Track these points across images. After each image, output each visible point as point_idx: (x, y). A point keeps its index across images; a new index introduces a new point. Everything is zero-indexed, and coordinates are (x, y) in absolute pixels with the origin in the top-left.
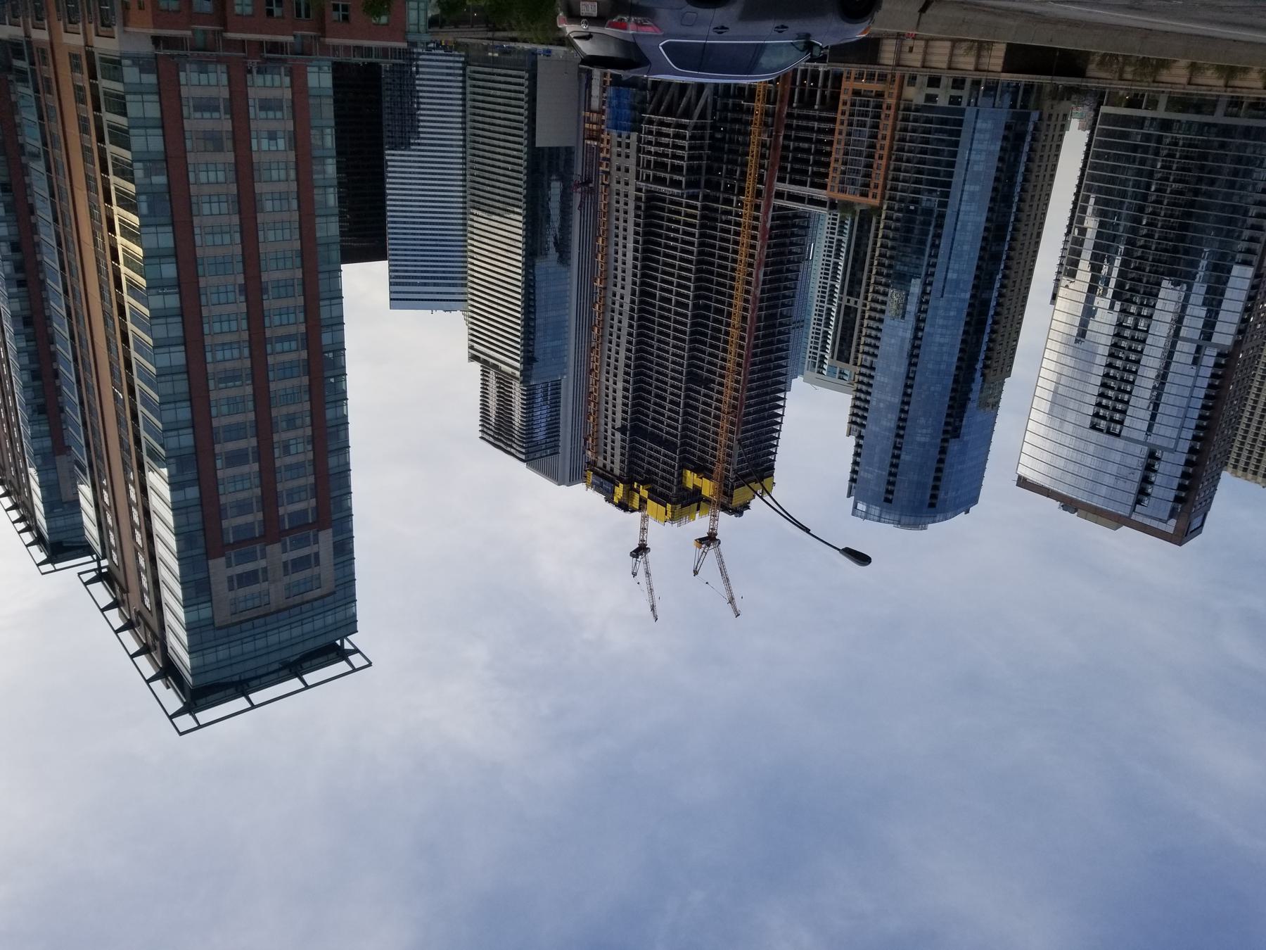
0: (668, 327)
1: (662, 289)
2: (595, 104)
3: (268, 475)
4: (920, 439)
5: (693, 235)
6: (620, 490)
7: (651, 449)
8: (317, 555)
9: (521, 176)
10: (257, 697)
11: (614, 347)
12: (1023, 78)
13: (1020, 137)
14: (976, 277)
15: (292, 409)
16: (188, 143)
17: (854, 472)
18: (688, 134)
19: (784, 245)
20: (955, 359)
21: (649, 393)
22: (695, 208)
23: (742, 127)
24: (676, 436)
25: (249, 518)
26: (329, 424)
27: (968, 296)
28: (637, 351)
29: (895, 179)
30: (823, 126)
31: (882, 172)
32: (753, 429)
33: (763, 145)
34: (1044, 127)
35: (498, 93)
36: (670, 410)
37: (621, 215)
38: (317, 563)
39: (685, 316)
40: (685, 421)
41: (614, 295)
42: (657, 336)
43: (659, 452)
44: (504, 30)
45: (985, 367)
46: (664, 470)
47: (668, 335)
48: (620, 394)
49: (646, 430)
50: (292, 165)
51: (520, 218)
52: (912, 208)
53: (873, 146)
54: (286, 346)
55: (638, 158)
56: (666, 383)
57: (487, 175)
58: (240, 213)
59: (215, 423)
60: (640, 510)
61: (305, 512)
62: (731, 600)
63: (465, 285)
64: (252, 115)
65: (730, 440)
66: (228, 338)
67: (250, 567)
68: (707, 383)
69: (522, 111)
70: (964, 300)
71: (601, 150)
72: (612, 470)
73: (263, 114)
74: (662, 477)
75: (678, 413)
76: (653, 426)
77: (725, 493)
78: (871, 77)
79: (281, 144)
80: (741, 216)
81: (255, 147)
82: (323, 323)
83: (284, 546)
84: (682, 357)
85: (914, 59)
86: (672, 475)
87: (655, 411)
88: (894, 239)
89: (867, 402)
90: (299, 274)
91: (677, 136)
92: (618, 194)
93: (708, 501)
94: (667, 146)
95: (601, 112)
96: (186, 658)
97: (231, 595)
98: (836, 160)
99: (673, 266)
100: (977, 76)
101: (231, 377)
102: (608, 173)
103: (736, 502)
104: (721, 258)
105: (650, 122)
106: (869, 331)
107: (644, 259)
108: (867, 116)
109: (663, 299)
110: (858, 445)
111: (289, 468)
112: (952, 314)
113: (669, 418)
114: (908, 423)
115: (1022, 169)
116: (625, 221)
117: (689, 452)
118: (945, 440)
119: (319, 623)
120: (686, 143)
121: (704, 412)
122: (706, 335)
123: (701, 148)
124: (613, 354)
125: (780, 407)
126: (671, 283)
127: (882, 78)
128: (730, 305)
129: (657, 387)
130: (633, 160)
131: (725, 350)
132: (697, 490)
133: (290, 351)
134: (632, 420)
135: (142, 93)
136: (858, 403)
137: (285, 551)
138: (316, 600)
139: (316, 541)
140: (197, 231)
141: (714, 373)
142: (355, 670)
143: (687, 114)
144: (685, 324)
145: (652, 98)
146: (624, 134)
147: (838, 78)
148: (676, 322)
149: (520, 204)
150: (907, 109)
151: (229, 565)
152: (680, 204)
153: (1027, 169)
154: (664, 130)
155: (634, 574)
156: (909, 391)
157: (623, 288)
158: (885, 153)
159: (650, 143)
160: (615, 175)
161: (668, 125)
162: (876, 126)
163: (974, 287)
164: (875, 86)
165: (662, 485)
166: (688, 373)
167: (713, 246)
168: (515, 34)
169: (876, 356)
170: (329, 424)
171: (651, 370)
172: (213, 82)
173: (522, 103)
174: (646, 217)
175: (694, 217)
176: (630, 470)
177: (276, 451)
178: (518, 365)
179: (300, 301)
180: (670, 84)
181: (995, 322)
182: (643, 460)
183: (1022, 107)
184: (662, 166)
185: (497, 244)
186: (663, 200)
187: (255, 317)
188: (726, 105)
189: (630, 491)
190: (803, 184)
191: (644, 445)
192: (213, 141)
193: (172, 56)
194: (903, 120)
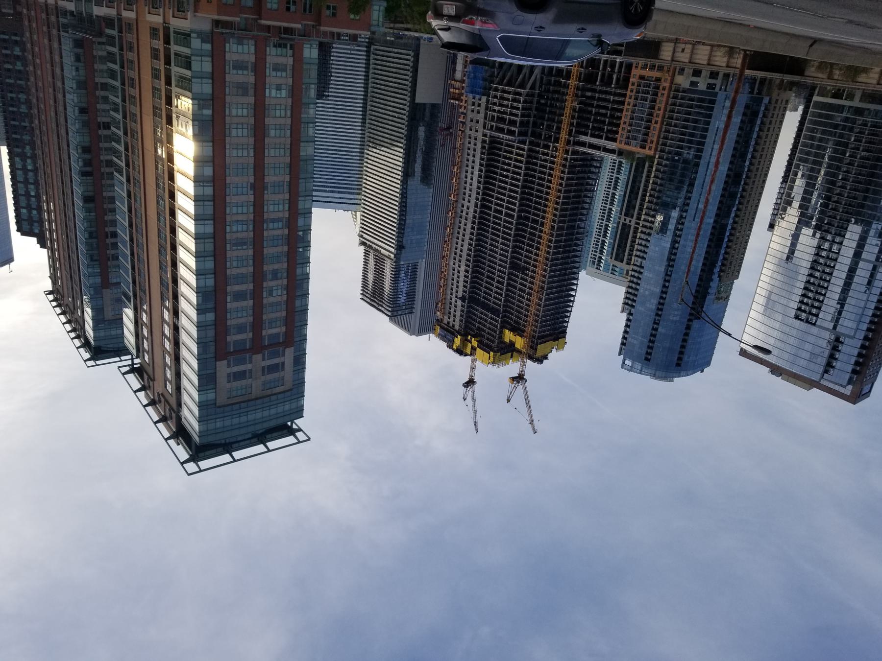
0: (499, 230)
1: (497, 204)
2: (458, 75)
3: (258, 310)
4: (671, 318)
5: (520, 168)
6: (458, 340)
7: (482, 313)
8: (283, 363)
9: (404, 122)
10: (237, 454)
11: (460, 241)
12: (760, 74)
13: (755, 114)
14: (719, 209)
15: (276, 266)
16: (227, 89)
17: (624, 338)
18: (522, 99)
19: (583, 178)
20: (701, 264)
22: (523, 150)
23: (560, 97)
24: (500, 306)
25: (243, 336)
26: (298, 278)
27: (712, 221)
28: (476, 245)
29: (666, 138)
30: (616, 98)
31: (657, 133)
33: (574, 110)
34: (772, 108)
35: (392, 65)
36: (497, 287)
37: (471, 152)
38: (283, 369)
39: (511, 223)
40: (507, 295)
41: (463, 206)
42: (490, 236)
43: (487, 316)
44: (402, 23)
45: (721, 271)
46: (489, 329)
47: (498, 236)
48: (462, 274)
49: (479, 300)
50: (289, 107)
51: (402, 150)
53: (651, 114)
54: (276, 225)
55: (486, 114)
57: (380, 120)
58: (255, 136)
59: (228, 272)
60: (471, 355)
61: (278, 334)
62: (532, 422)
63: (359, 194)
64: (268, 74)
65: (538, 310)
66: (240, 218)
67: (241, 368)
68: (524, 270)
69: (407, 78)
70: (709, 224)
71: (461, 107)
72: (453, 326)
73: (274, 73)
74: (488, 333)
75: (502, 290)
76: (484, 298)
77: (532, 347)
78: (653, 67)
79: (284, 92)
80: (555, 157)
81: (267, 95)
82: (300, 212)
83: (264, 356)
84: (508, 252)
85: (684, 57)
86: (495, 332)
87: (486, 287)
88: (662, 179)
89: (637, 290)
90: (287, 178)
91: (514, 100)
92: (470, 138)
93: (519, 352)
94: (507, 106)
95: (463, 81)
96: (196, 425)
97: (228, 385)
98: (625, 123)
99: (505, 189)
100: (728, 70)
101: (240, 243)
102: (463, 123)
103: (539, 354)
104: (539, 184)
105: (496, 90)
106: (640, 241)
107: (485, 183)
109: (496, 211)
110: (628, 320)
111: (272, 305)
113: (496, 292)
114: (665, 306)
115: (755, 136)
116: (474, 156)
117: (508, 317)
118: (690, 320)
119: (280, 409)
120: (520, 106)
121: (520, 290)
122: (525, 237)
123: (530, 109)
124: (459, 246)
125: (573, 290)
126: (503, 200)
127: (661, 68)
128: (543, 218)
129: (488, 271)
130: (482, 115)
131: (538, 249)
132: (512, 344)
133: (278, 229)
134: (470, 292)
135: (201, 56)
136: (630, 290)
137: (264, 359)
138: (280, 393)
139: (284, 355)
140: (228, 146)
141: (529, 264)
142: (299, 442)
143: (522, 86)
144: (511, 229)
145: (498, 74)
146: (478, 97)
147: (629, 67)
148: (504, 227)
149: (402, 141)
150: (677, 90)
151: (229, 366)
152: (513, 147)
153: (759, 137)
154: (506, 95)
155: (465, 399)
156: (667, 284)
157: (469, 202)
158: (659, 120)
159: (495, 104)
160: (469, 124)
161: (509, 93)
162: (654, 101)
163: (717, 215)
164: (656, 74)
165: (488, 339)
166: (511, 263)
167: (534, 177)
168: (409, 26)
170: (298, 278)
171: (485, 259)
172: (246, 51)
173: (409, 73)
174: (488, 154)
175: (522, 156)
176: (466, 326)
177: (265, 293)
178: (393, 250)
179: (287, 196)
180: (511, 65)
181: (729, 241)
182: (475, 320)
183: (758, 94)
184: (501, 120)
185: (385, 166)
186: (501, 144)
187: (258, 206)
188: (550, 81)
189: (465, 341)
190: (600, 137)
191: (477, 310)
192: (242, 89)
193: (222, 33)
194: (673, 98)
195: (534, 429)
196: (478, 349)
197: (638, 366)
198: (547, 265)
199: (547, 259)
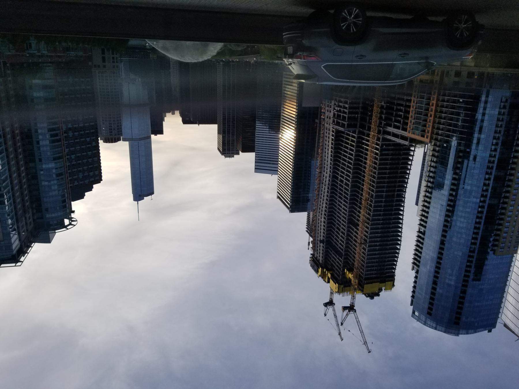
6: (320, 270)
17: (414, 292)
21: (335, 226)
22: (354, 137)
24: (342, 250)
27: (478, 200)
32: (378, 254)
33: (382, 107)
43: (336, 256)
46: (337, 266)
49: (333, 244)
52: (445, 145)
53: (427, 110)
56: (340, 222)
60: (329, 282)
70: (476, 203)
86: (340, 269)
88: (436, 162)
91: (346, 103)
98: (412, 117)
102: (324, 119)
108: (424, 93)
110: (416, 277)
123: (358, 108)
132: (350, 280)
134: (327, 237)
158: (433, 113)
165: (336, 274)
166: (349, 219)
169: (425, 227)
184: (339, 116)
190: (397, 127)
197: (423, 318)
198: (368, 224)
199: (368, 219)
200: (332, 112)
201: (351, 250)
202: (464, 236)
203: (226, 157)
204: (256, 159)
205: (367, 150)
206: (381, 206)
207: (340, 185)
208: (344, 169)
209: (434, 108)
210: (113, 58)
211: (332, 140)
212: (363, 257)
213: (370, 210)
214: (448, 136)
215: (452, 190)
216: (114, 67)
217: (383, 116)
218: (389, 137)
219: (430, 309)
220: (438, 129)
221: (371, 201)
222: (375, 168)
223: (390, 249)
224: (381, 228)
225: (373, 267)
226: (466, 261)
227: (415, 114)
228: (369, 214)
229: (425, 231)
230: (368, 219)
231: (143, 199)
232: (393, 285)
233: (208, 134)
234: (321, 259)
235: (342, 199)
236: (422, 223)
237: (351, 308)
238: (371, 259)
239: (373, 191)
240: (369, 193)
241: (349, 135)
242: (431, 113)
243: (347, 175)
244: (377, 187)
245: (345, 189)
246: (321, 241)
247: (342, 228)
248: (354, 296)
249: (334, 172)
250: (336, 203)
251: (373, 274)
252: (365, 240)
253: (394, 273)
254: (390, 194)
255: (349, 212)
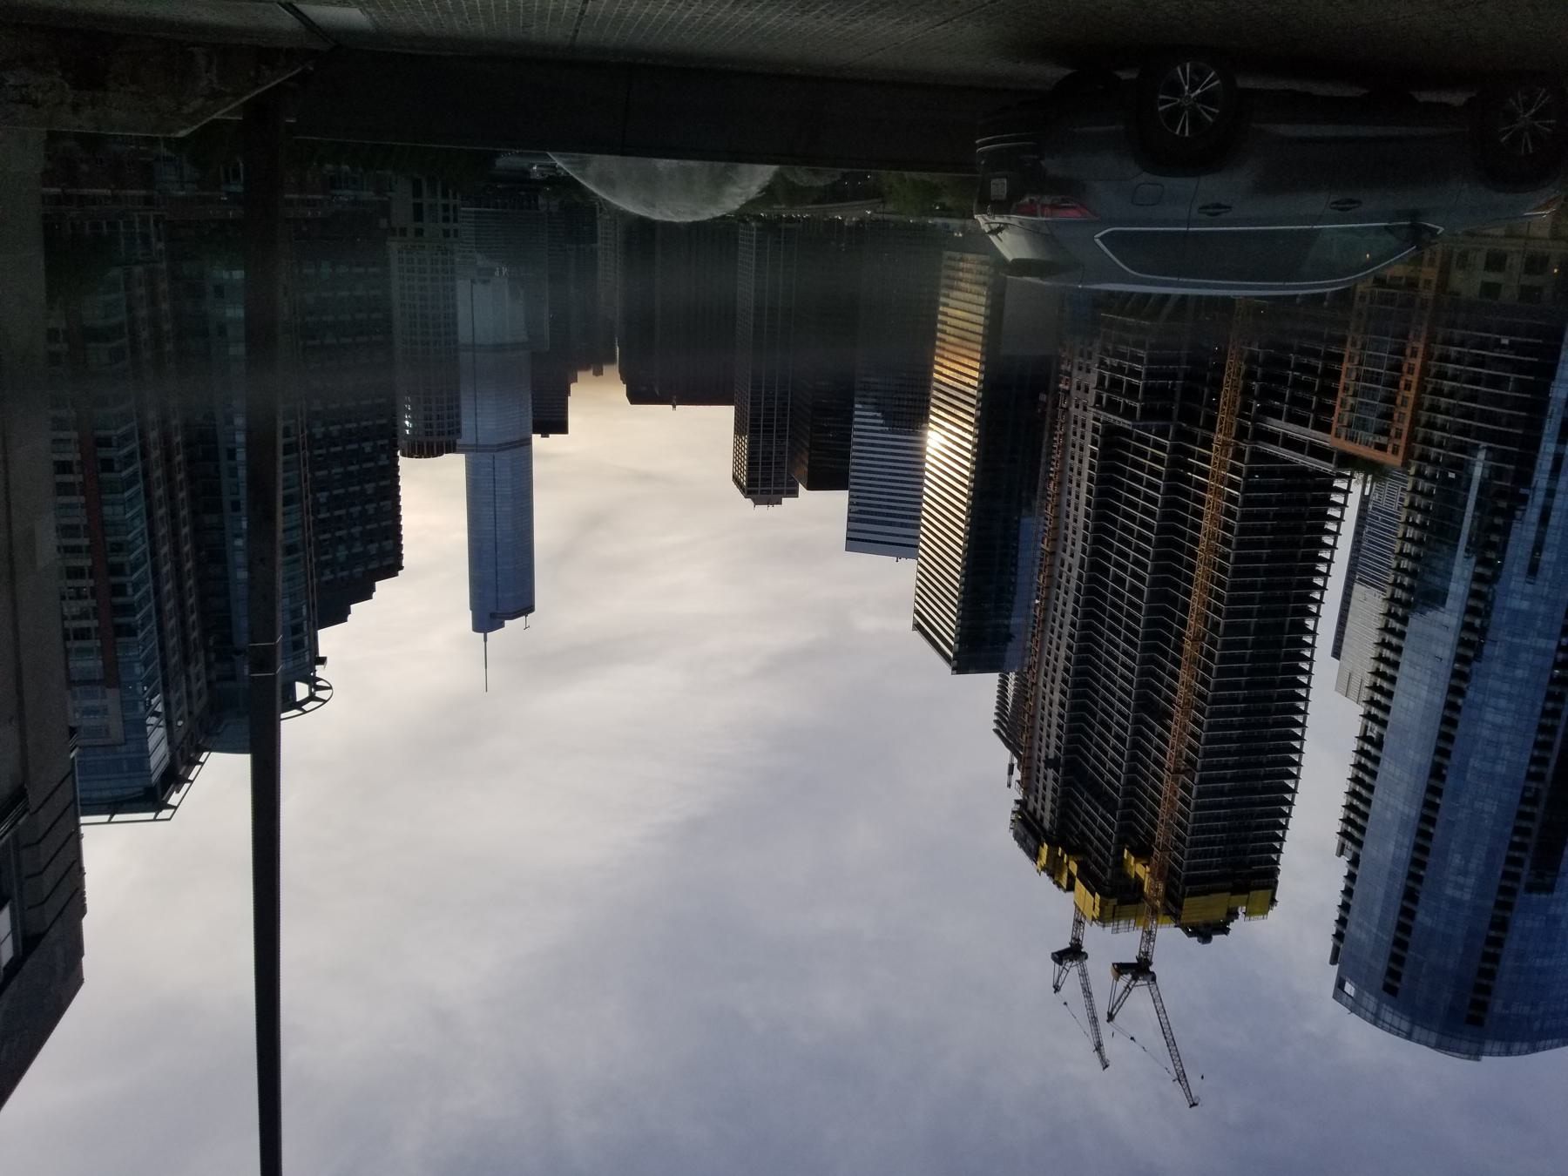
6: (1044, 850)
17: (1342, 922)
21: (1094, 715)
22: (1162, 448)
24: (1116, 790)
27: (1553, 645)
31: (1408, 412)
33: (1252, 359)
43: (1096, 810)
52: (1452, 475)
53: (1397, 367)
56: (1112, 706)
60: (1071, 888)
72: (1042, 818)
86: (1108, 849)
98: (1346, 389)
102: (1068, 393)
110: (1351, 877)
112: (1519, 673)
116: (1081, 461)
117: (1136, 820)
132: (1139, 883)
134: (1067, 751)
158: (1414, 378)
165: (1096, 863)
166: (1138, 697)
169: (1383, 724)
184: (1115, 385)
190: (1303, 422)
195: (1188, 1094)
196: (1078, 882)
197: (1370, 1002)
198: (1201, 711)
199: (1201, 696)
200: (1095, 369)
201: (1145, 791)
202: (1506, 753)
203: (757, 503)
204: (850, 511)
205: (1203, 487)
206: (1241, 659)
207: (1115, 593)
208: (1128, 544)
209: (1418, 362)
210: (446, 208)
211: (1093, 455)
212: (1181, 812)
213: (1207, 669)
214: (1462, 448)
215: (1470, 610)
216: (446, 234)
217: (1256, 385)
218: (1272, 449)
219: (1393, 974)
220: (1431, 425)
221: (1213, 643)
222: (1226, 542)
223: (1267, 790)
224: (1241, 726)
225: (1213, 843)
226: (1509, 830)
227: (1357, 379)
228: (1205, 683)
229: (1381, 736)
230: (1201, 696)
231: (502, 625)
232: (1273, 901)
233: (706, 434)
234: (1047, 815)
235: (1118, 634)
236: (1374, 711)
237: (1140, 969)
238: (1208, 819)
239: (1217, 611)
240: (1207, 617)
241: (1146, 441)
242: (1409, 378)
243: (1137, 562)
244: (1232, 601)
245: (1131, 603)
246: (1050, 763)
247: (1118, 724)
248: (1150, 933)
249: (1095, 552)
250: (1100, 647)
251: (1209, 866)
252: (1188, 760)
253: (1277, 863)
254: (1270, 620)
255: (1142, 673)
